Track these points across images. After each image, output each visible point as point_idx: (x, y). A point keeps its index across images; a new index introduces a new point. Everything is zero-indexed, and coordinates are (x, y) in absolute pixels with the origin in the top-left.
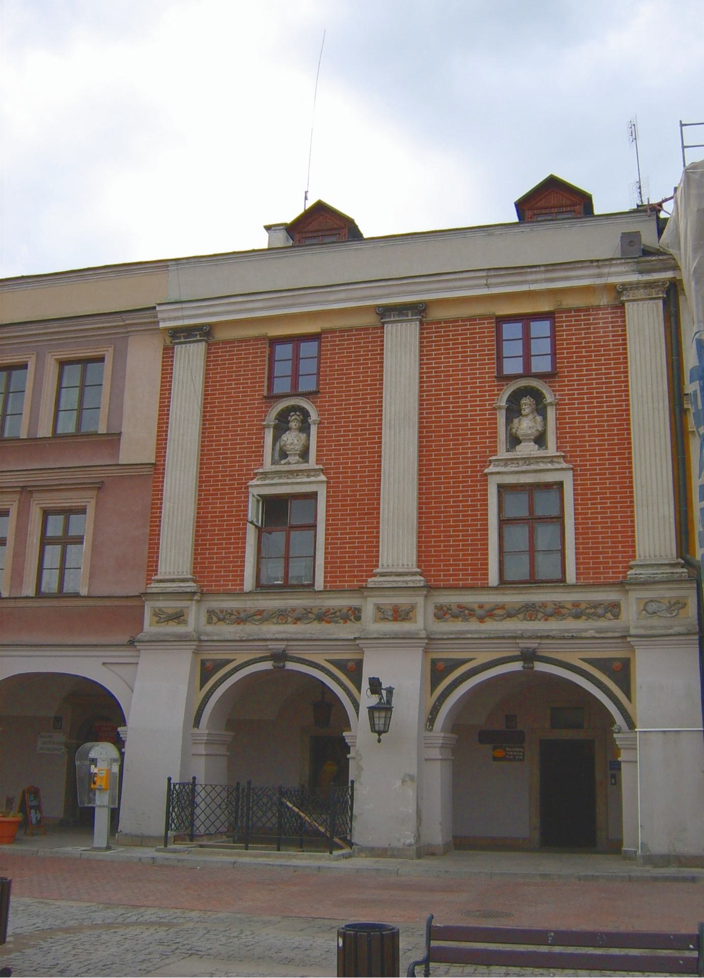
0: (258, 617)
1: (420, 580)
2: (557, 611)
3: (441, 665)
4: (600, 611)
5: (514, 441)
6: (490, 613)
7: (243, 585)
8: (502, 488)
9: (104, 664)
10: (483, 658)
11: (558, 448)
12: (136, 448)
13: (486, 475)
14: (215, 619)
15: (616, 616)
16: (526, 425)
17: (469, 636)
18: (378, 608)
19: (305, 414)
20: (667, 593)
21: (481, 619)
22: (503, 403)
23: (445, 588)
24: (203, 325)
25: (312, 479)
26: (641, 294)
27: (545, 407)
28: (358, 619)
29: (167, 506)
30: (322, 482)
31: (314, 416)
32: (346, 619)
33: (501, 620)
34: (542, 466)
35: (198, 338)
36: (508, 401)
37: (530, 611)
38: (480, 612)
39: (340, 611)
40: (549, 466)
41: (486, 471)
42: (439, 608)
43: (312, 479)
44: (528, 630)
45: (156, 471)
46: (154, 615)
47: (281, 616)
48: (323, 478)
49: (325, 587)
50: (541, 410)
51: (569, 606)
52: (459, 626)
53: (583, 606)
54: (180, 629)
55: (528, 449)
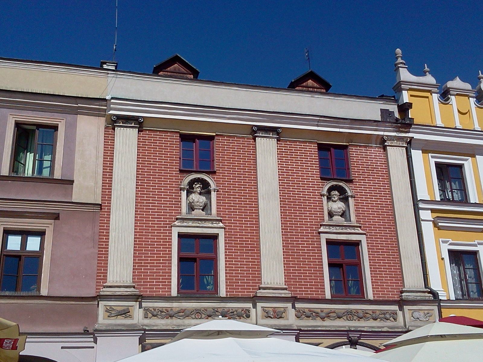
0: (181, 314)
2: (364, 316)
4: (388, 316)
6: (328, 316)
7: (170, 292)
8: (329, 243)
9: (62, 348)
13: (319, 233)
14: (150, 315)
17: (320, 329)
19: (205, 185)
24: (139, 117)
26: (395, 143)
27: (348, 197)
29: (112, 235)
30: (222, 228)
31: (213, 186)
33: (334, 320)
34: (349, 231)
35: (133, 125)
37: (350, 315)
38: (323, 314)
39: (236, 311)
40: (353, 231)
41: (320, 230)
43: (215, 225)
44: (352, 327)
45: (100, 209)
46: (106, 311)
48: (221, 225)
49: (227, 295)
51: (371, 312)
53: (378, 312)
54: (128, 322)
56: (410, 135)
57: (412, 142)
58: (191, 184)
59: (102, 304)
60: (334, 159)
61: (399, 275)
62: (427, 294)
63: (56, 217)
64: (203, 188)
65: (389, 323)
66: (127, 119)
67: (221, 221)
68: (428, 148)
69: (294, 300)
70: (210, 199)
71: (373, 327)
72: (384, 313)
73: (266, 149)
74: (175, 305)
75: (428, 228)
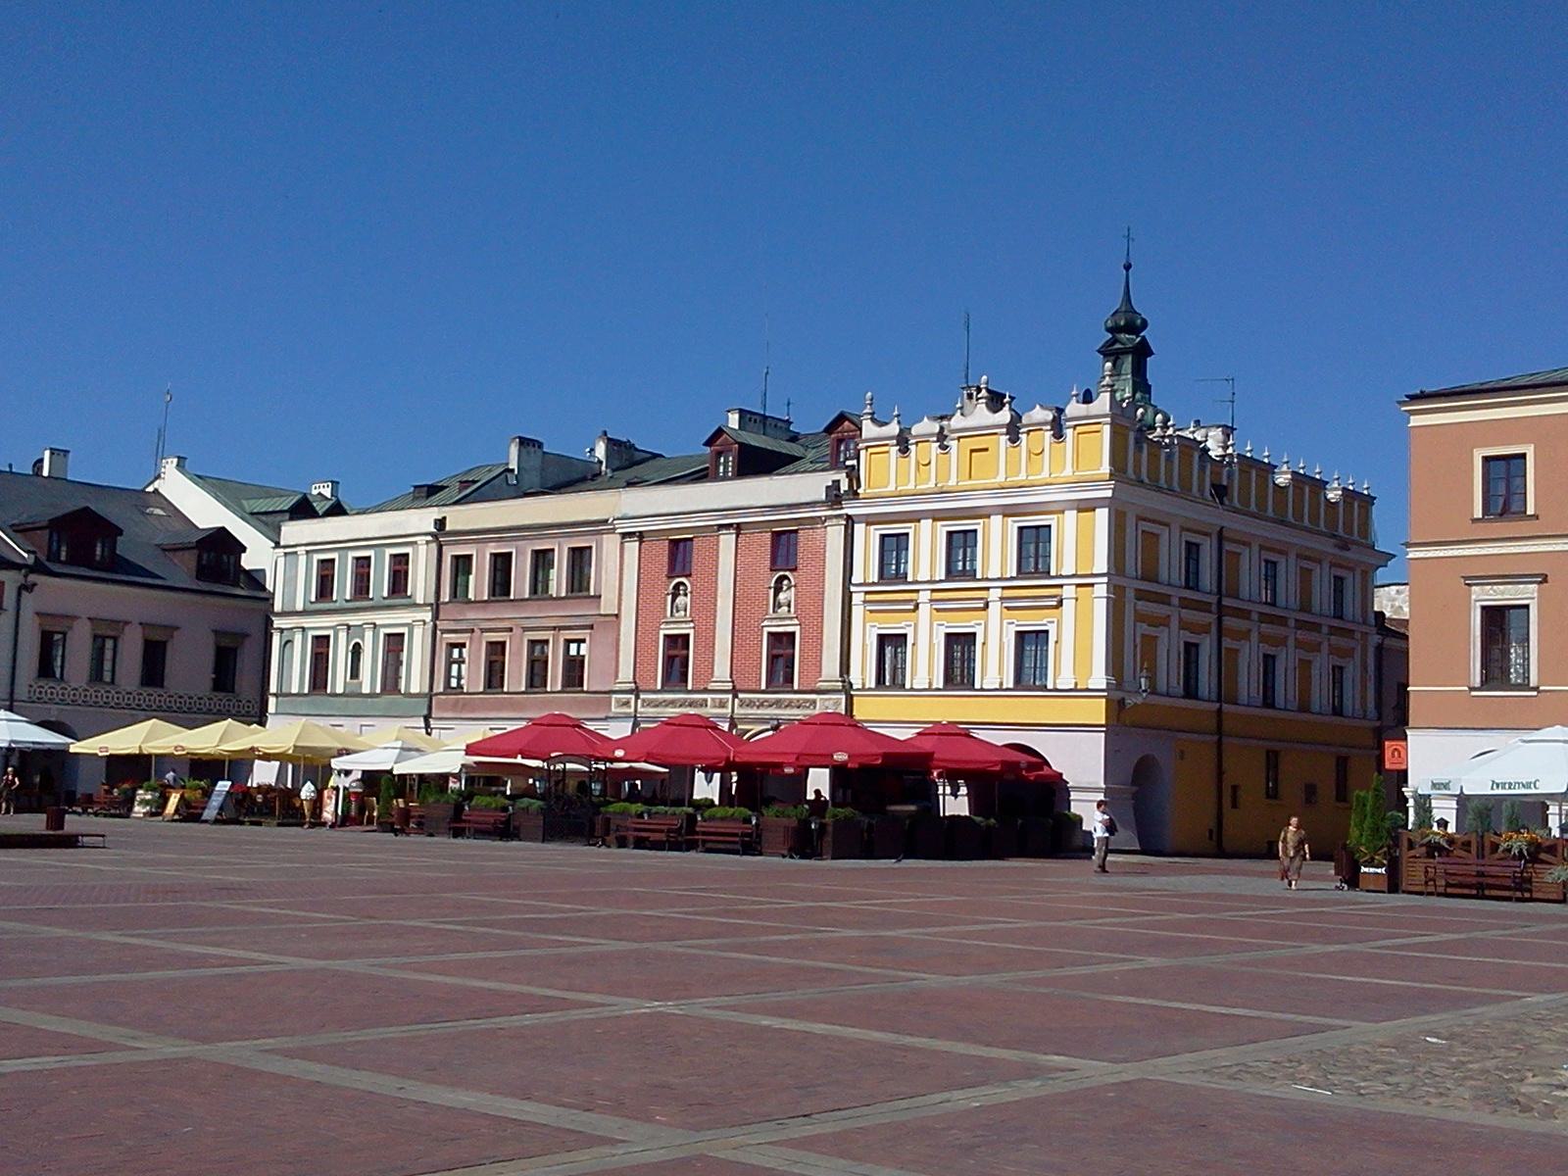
2: (789, 704)
5: (777, 605)
6: (761, 705)
12: (607, 606)
15: (815, 707)
22: (772, 585)
25: (688, 626)
26: (835, 521)
32: (701, 705)
36: (776, 582)
37: (778, 703)
47: (672, 703)
48: (692, 625)
59: (614, 696)
60: (784, 546)
63: (591, 627)
66: (631, 534)
68: (870, 520)
72: (807, 701)
74: (660, 696)
75: (857, 612)
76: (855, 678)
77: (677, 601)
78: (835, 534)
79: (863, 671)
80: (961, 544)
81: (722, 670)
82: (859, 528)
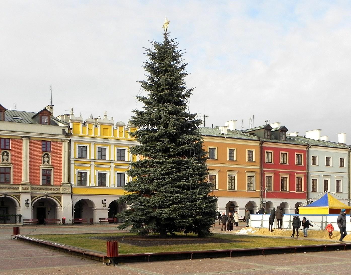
1: (29, 183)
3: (33, 197)
5: (44, 162)
6: (40, 189)
8: (42, 170)
10: (39, 196)
11: (51, 164)
15: (59, 190)
16: (46, 159)
18: (23, 187)
19: (7, 153)
20: (67, 187)
21: (39, 190)
23: (33, 185)
25: (10, 165)
27: (49, 157)
28: (19, 189)
31: (10, 154)
32: (17, 189)
34: (49, 167)
37: (46, 189)
40: (50, 167)
42: (32, 188)
43: (10, 165)
48: (12, 165)
50: (48, 157)
52: (36, 191)
55: (46, 163)
56: (70, 139)
57: (71, 141)
58: (3, 153)
61: (61, 180)
62: (69, 184)
64: (7, 154)
65: (57, 191)
67: (12, 164)
69: (31, 185)
70: (8, 157)
71: (52, 192)
73: (26, 144)
76: (72, 182)
77: (3, 157)
78: (65, 145)
79: (75, 180)
80: (102, 152)
81: (25, 178)
82: (72, 144)
